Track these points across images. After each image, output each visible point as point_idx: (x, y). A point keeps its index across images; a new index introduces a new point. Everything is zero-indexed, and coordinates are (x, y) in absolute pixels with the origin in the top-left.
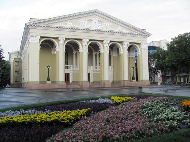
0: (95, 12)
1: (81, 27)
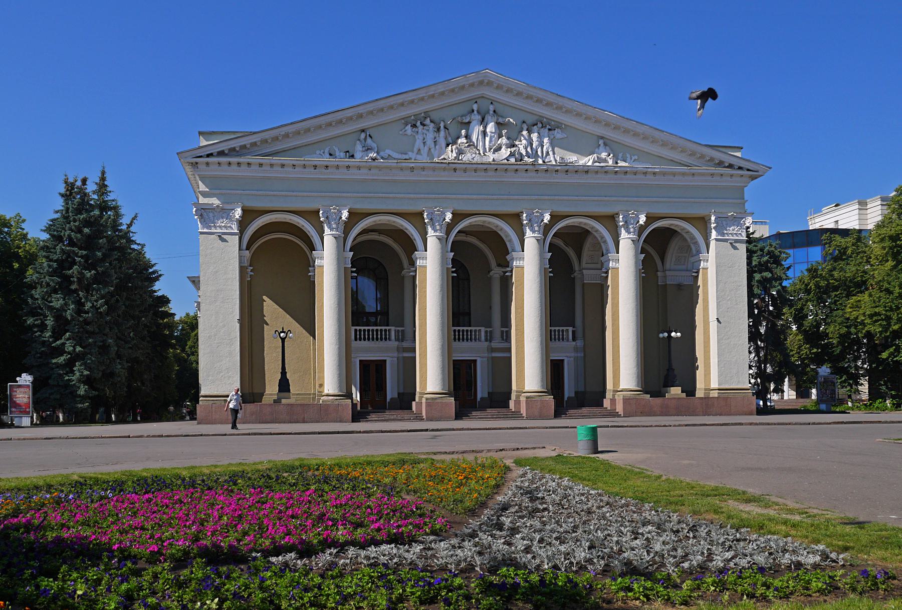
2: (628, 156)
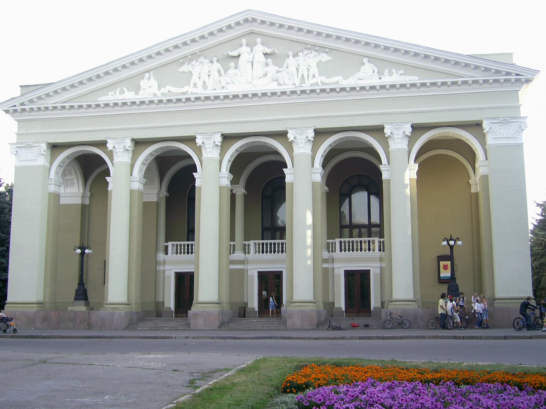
0: (246, 20)
1: (195, 90)
2: (394, 71)
